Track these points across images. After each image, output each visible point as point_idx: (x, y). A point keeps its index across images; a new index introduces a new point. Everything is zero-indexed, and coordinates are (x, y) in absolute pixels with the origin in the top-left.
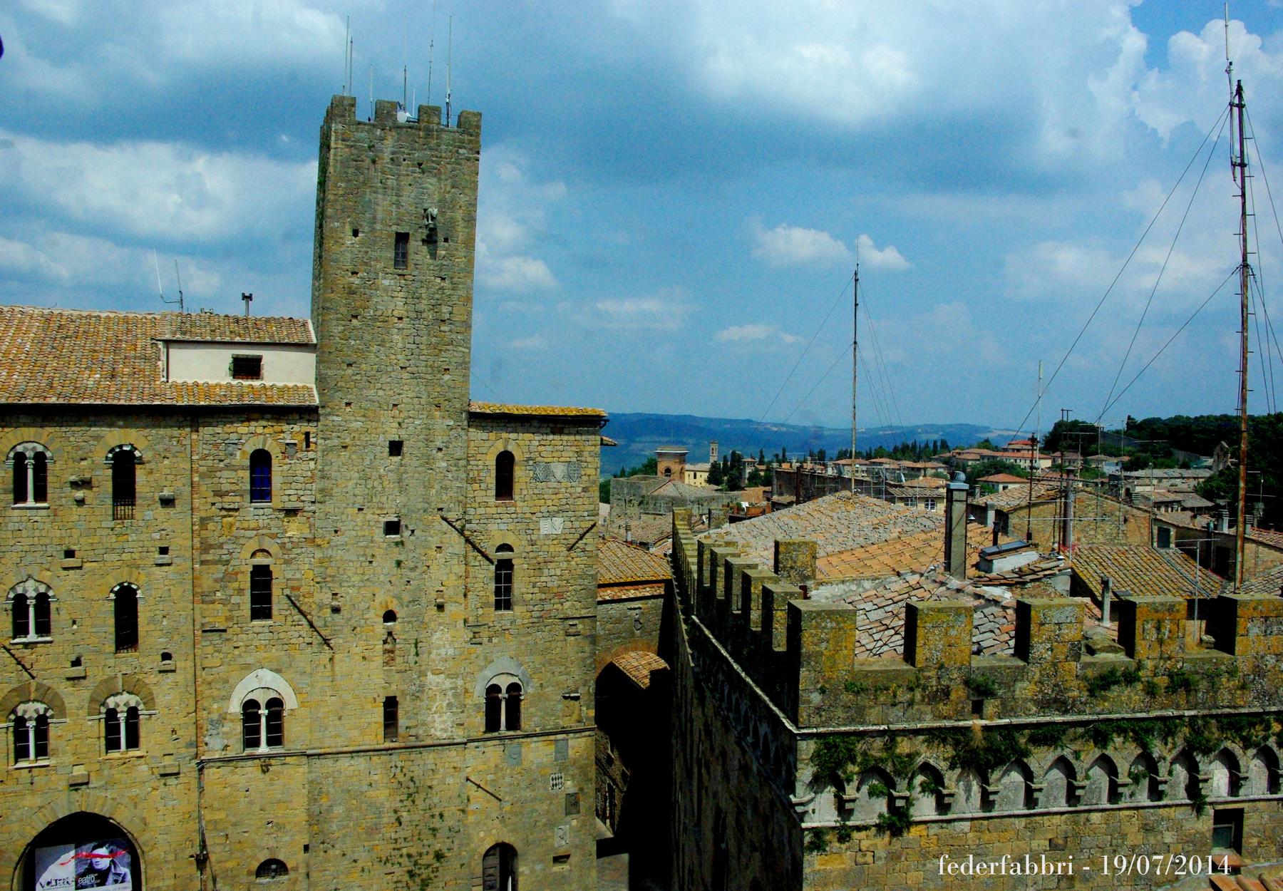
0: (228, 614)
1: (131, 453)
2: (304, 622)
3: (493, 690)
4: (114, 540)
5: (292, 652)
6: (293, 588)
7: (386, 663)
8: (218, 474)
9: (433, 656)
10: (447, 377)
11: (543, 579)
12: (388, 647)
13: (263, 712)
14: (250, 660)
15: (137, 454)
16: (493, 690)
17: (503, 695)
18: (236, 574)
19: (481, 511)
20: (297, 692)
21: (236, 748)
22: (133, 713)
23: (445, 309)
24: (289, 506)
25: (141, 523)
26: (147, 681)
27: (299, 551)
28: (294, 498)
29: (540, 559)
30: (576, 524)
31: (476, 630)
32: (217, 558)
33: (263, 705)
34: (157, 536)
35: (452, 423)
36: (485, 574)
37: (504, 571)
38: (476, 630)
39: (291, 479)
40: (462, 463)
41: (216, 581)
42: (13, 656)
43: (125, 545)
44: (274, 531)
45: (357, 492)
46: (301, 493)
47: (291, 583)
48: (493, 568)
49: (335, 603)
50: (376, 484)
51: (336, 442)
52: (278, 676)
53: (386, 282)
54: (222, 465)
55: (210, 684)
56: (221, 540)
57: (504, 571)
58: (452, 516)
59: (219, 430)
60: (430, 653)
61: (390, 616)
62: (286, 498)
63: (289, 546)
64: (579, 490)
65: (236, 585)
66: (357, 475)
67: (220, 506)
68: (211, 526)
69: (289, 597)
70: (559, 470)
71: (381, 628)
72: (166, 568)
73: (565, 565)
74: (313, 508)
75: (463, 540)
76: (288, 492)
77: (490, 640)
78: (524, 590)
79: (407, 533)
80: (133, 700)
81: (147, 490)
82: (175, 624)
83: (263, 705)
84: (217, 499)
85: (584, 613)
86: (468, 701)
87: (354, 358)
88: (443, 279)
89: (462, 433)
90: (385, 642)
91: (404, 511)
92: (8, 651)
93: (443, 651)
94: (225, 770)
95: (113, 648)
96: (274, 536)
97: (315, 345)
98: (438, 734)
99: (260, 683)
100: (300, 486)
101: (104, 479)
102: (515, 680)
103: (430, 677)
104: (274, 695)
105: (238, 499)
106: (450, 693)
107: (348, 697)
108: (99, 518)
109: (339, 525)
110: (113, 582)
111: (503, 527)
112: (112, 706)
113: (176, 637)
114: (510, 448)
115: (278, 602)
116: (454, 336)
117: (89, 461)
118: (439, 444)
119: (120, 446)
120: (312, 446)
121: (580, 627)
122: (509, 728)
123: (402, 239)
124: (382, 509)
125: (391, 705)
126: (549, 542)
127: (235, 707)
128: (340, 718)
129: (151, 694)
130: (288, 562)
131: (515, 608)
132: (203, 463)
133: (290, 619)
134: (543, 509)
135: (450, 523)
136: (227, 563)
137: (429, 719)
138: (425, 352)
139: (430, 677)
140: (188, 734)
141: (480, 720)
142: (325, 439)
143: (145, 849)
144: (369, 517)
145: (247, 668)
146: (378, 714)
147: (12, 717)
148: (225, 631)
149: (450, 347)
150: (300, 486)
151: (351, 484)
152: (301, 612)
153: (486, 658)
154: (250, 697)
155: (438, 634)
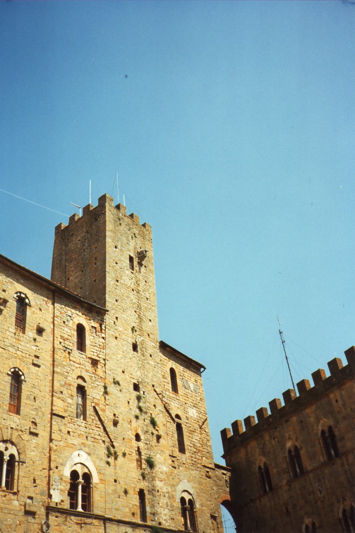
0: (66, 408)
2: (100, 426)
3: (183, 500)
4: (14, 340)
5: (95, 444)
6: (96, 404)
8: (63, 328)
10: (150, 323)
11: (194, 440)
13: (81, 480)
14: (75, 442)
15: (27, 301)
16: (183, 500)
18: (70, 385)
19: (167, 393)
21: (66, 505)
22: (12, 456)
25: (27, 338)
26: (22, 436)
27: (98, 383)
28: (96, 354)
29: (191, 429)
30: (201, 416)
32: (62, 372)
33: (81, 477)
34: (34, 348)
38: (173, 459)
39: (94, 344)
41: (61, 386)
43: (20, 347)
44: (87, 368)
46: (98, 352)
47: (95, 401)
48: (175, 425)
51: (113, 333)
52: (89, 458)
55: (55, 451)
56: (64, 363)
57: (179, 428)
61: (138, 438)
62: (92, 353)
64: (199, 399)
65: (70, 392)
66: (121, 353)
67: (63, 345)
68: (59, 353)
69: (94, 407)
70: (192, 386)
71: (135, 443)
72: (37, 368)
73: (200, 436)
76: (93, 350)
77: (179, 468)
78: (188, 444)
81: (31, 321)
82: (40, 404)
83: (81, 477)
84: (62, 341)
85: (210, 466)
86: (174, 504)
91: (140, 380)
94: (61, 519)
95: (7, 408)
96: (87, 371)
100: (98, 349)
101: (13, 305)
104: (86, 471)
105: (71, 345)
106: (167, 495)
108: (9, 325)
110: (7, 367)
111: (176, 405)
113: (40, 413)
114: (174, 367)
115: (90, 411)
117: (7, 292)
119: (20, 293)
120: (103, 331)
121: (210, 474)
123: (131, 259)
126: (193, 421)
127: (67, 473)
128: (119, 497)
129: (24, 447)
130: (92, 388)
131: (187, 452)
134: (188, 402)
135: (158, 394)
137: (159, 510)
140: (42, 484)
142: (109, 330)
144: (127, 377)
145: (73, 446)
148: (63, 417)
150: (98, 349)
151: (119, 356)
152: (100, 420)
153: (179, 479)
154: (74, 468)
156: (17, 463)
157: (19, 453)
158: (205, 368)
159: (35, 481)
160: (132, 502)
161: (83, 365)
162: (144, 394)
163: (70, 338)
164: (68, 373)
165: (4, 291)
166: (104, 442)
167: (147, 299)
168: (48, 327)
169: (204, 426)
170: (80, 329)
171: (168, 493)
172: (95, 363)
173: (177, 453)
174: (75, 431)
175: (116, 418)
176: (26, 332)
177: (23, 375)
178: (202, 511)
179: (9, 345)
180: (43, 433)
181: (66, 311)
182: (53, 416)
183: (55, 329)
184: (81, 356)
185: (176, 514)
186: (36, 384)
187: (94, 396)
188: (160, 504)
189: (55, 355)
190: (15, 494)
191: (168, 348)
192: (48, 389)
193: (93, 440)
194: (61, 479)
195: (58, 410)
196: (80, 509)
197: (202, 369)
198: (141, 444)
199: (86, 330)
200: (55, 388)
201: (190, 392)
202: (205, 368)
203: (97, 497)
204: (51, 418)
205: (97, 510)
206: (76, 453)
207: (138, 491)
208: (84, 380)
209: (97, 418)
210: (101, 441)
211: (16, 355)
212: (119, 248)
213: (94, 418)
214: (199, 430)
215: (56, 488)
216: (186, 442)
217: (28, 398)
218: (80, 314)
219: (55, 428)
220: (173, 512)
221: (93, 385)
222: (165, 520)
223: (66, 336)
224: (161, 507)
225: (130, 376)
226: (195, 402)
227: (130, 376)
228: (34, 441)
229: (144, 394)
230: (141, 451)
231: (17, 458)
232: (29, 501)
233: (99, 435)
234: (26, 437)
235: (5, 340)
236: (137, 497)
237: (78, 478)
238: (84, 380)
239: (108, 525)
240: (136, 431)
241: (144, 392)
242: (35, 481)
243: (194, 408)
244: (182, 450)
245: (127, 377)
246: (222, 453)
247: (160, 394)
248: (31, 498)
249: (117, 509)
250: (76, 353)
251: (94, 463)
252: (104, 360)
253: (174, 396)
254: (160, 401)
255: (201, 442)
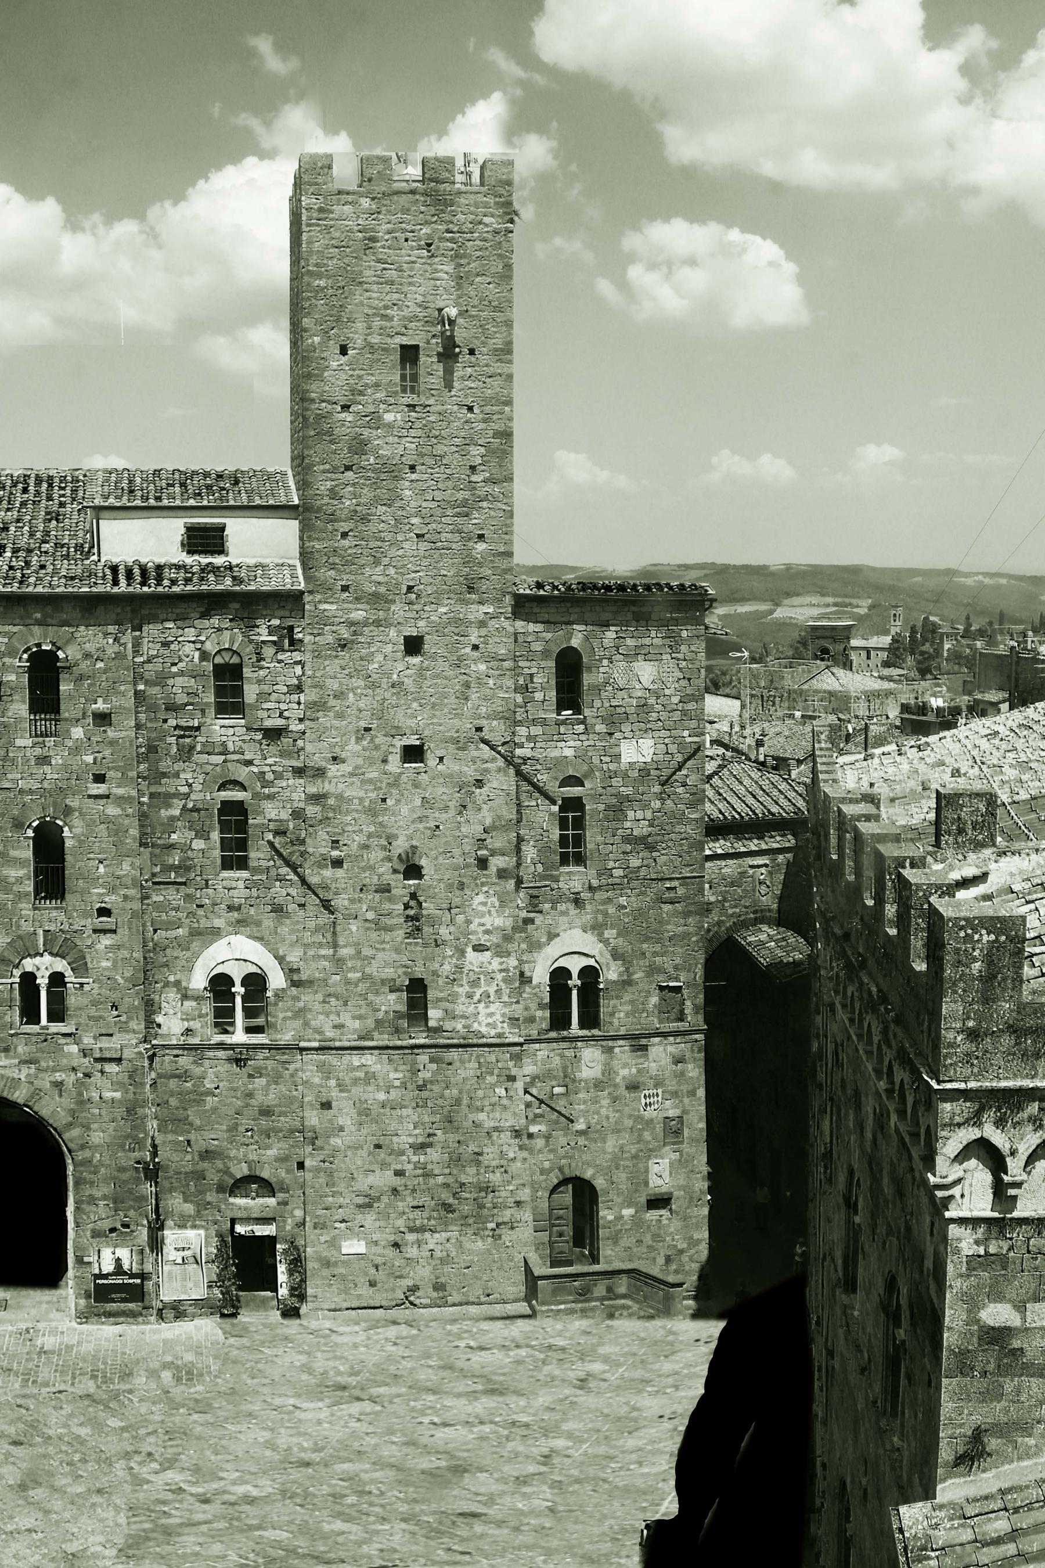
1: (52, 655)
2: (292, 876)
7: (409, 935)
8: (170, 682)
9: (472, 927)
10: (481, 547)
12: (412, 912)
16: (559, 975)
17: (575, 981)
24: (269, 723)
27: (284, 784)
31: (535, 892)
35: (491, 610)
36: (544, 817)
37: (572, 811)
40: (507, 664)
44: (248, 756)
45: (362, 705)
48: (555, 809)
49: (335, 853)
50: (387, 695)
51: (330, 639)
53: (389, 417)
54: (174, 669)
57: (572, 811)
58: (497, 739)
59: (171, 625)
60: (468, 922)
63: (270, 776)
74: (301, 727)
75: (512, 771)
76: (265, 706)
79: (432, 761)
88: (470, 409)
89: (506, 624)
90: (407, 907)
93: (488, 921)
97: (296, 507)
98: (484, 1030)
102: (591, 962)
103: (470, 954)
106: (499, 976)
109: (337, 749)
118: (474, 640)
119: (39, 645)
122: (582, 1025)
132: (147, 666)
133: (273, 872)
135: (493, 748)
136: (187, 796)
139: (470, 954)
141: (544, 1016)
149: (485, 504)
155: (481, 898)
166: (302, 906)
167: (473, 468)
171: (506, 970)
181: (180, 632)
184: (231, 731)
188: (476, 998)
209: (279, 862)
213: (272, 863)
220: (520, 1006)
222: (488, 1025)
223: (182, 698)
224: (479, 1001)
225: (393, 732)
230: (421, 899)
233: (288, 895)
241: (441, 759)
247: (504, 744)
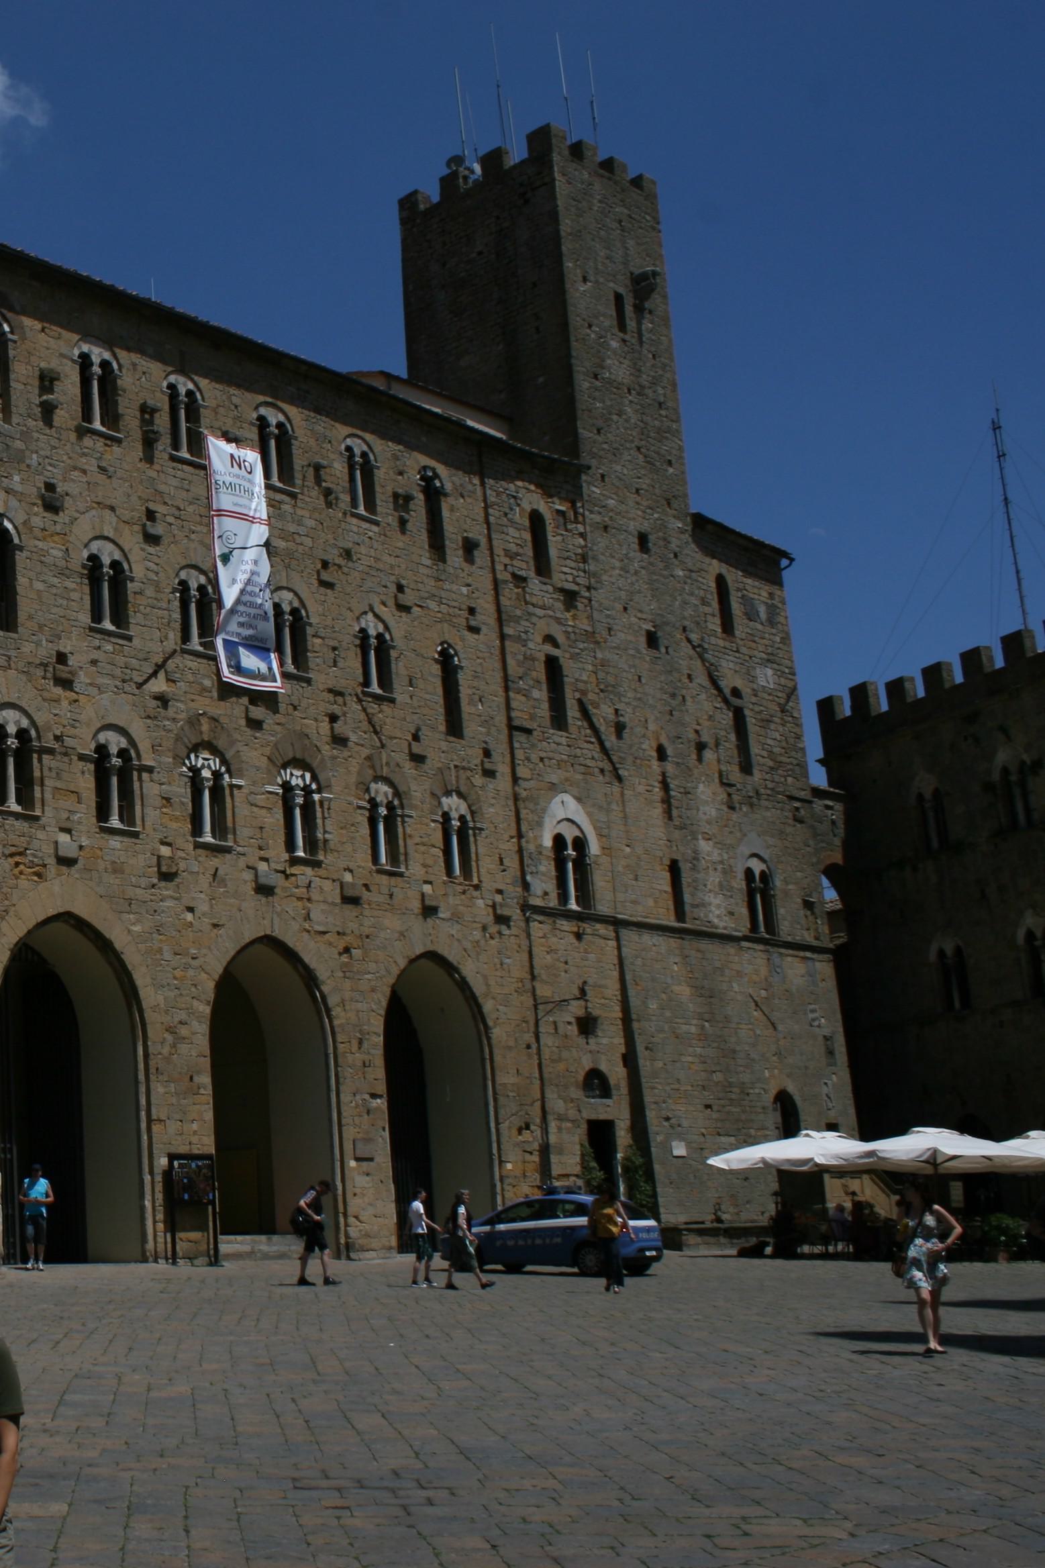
3: (749, 873)
11: (770, 742)
13: (571, 852)
14: (554, 778)
16: (749, 873)
19: (713, 640)
20: (600, 836)
21: (553, 902)
23: (660, 391)
28: (570, 578)
30: (783, 681)
34: (464, 590)
42: (364, 710)
46: (575, 572)
47: (581, 686)
48: (731, 714)
58: (694, 637)
61: (661, 754)
64: (778, 639)
66: (618, 564)
76: (565, 569)
78: (757, 751)
80: (463, 809)
84: (507, 561)
85: (802, 794)
87: (600, 423)
92: (360, 701)
99: (564, 812)
104: (578, 833)
105: (524, 566)
106: (720, 867)
107: (639, 850)
109: (611, 621)
111: (731, 665)
112: (446, 809)
113: (493, 729)
115: (572, 712)
116: (669, 423)
120: (580, 519)
121: (802, 812)
124: (641, 611)
125: (674, 869)
127: (548, 842)
128: (636, 880)
131: (755, 772)
134: (756, 653)
135: (694, 647)
137: (706, 898)
138: (652, 435)
143: (490, 1023)
145: (554, 788)
146: (663, 882)
147: (367, 797)
154: (556, 831)
156: (471, 832)
157: (473, 813)
158: (792, 560)
159: (501, 860)
160: (659, 887)
161: (549, 609)
162: (667, 653)
163: (521, 551)
164: (526, 632)
165: (401, 473)
168: (477, 533)
169: (791, 704)
170: (536, 520)
171: (721, 862)
172: (570, 598)
173: (735, 775)
174: (551, 755)
175: (621, 719)
176: (448, 558)
177: (456, 654)
178: (786, 893)
179: (426, 595)
180: (503, 769)
182: (515, 733)
183: (493, 536)
184: (545, 588)
185: (737, 904)
186: (479, 669)
187: (577, 676)
188: (709, 887)
189: (501, 598)
190: (477, 887)
191: (710, 527)
192: (499, 676)
193: (582, 769)
194: (540, 853)
195: (520, 718)
196: (573, 906)
197: (784, 562)
198: (670, 768)
199: (547, 523)
200: (510, 672)
201: (760, 627)
202: (792, 560)
203: (600, 881)
204: (511, 737)
205: (603, 907)
206: (558, 799)
207: (668, 863)
208: (556, 645)
210: (597, 770)
211: (439, 615)
212: (592, 278)
213: (580, 723)
214: (779, 714)
215: (534, 870)
216: (755, 749)
217: (471, 702)
218: (532, 487)
219: (519, 754)
221: (572, 650)
222: (718, 916)
224: (710, 891)
225: (639, 615)
226: (770, 650)
227: (639, 615)
228: (491, 786)
229: (667, 653)
231: (471, 824)
232: (498, 898)
233: (593, 758)
234: (478, 780)
235: (420, 586)
236: (667, 875)
237: (566, 849)
238: (556, 645)
239: (625, 933)
240: (658, 739)
241: (667, 648)
242: (501, 860)
243: (769, 665)
244: (746, 768)
245: (633, 619)
246: (821, 755)
248: (500, 892)
249: (634, 902)
250: (535, 584)
251: (589, 815)
252: (589, 588)
253: (727, 644)
254: (699, 663)
255: (784, 744)
